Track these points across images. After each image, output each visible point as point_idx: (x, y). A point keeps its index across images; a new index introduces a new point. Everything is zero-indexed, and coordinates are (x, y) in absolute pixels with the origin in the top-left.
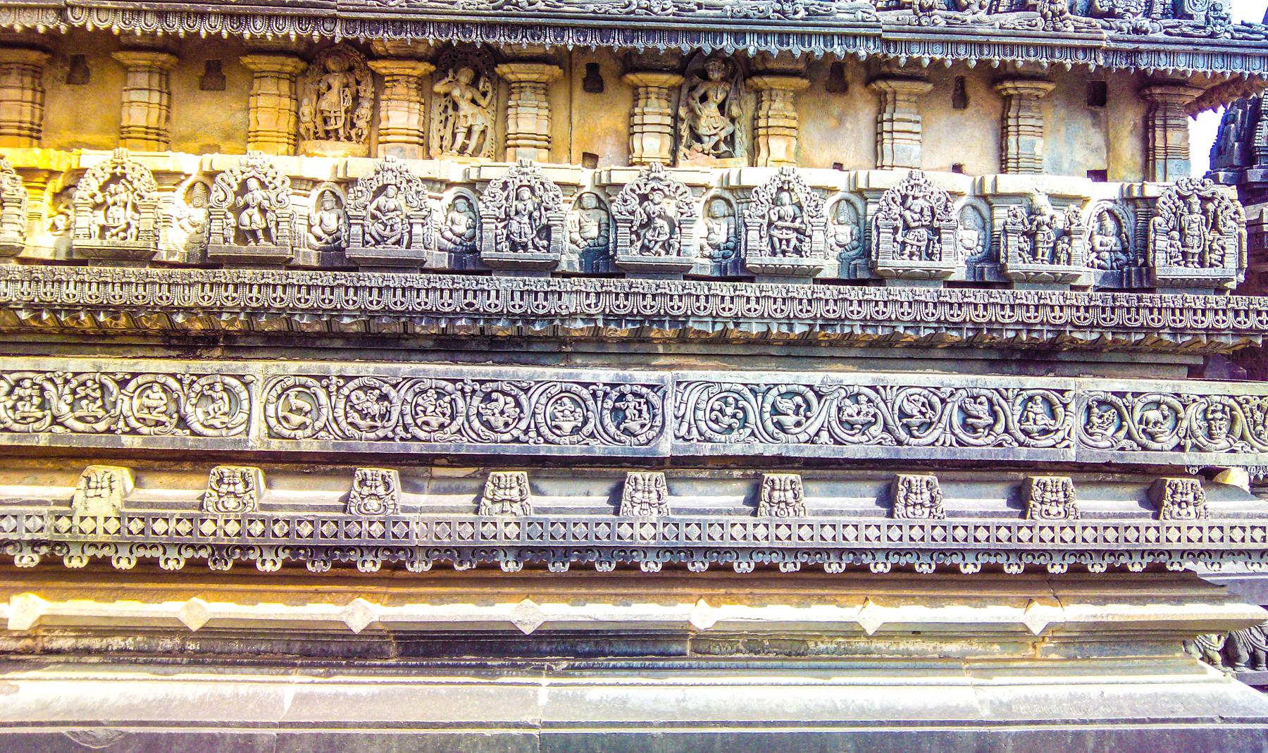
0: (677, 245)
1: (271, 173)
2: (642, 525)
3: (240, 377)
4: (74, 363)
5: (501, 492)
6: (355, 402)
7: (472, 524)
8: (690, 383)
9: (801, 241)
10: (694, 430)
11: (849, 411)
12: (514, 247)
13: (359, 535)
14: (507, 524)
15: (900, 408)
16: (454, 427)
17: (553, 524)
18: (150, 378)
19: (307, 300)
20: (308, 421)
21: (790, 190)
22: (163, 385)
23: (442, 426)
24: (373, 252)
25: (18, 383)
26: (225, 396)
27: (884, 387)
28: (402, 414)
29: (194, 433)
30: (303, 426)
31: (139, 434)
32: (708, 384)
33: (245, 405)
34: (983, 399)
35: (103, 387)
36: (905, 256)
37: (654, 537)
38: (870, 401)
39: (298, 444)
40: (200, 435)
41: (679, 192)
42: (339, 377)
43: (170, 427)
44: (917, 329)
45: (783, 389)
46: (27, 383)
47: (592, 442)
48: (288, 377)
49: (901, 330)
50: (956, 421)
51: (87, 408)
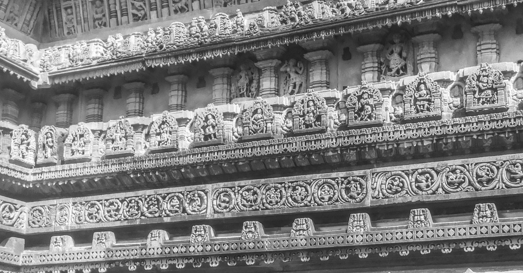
0: (374, 115)
1: (216, 111)
2: (357, 236)
3: (203, 191)
4: (149, 192)
5: (299, 226)
6: (244, 195)
7: (288, 241)
8: (378, 173)
9: (430, 105)
10: (381, 194)
11: (451, 177)
12: (307, 126)
13: (245, 248)
14: (301, 240)
15: (476, 174)
16: (282, 202)
17: (320, 238)
18: (173, 194)
19: (225, 156)
20: (227, 205)
21: (424, 83)
22: (178, 197)
23: (277, 203)
24: (252, 136)
25: (130, 202)
26: (199, 199)
27: (468, 165)
28: (262, 199)
29: (188, 214)
30: (226, 208)
31: (170, 216)
32: (386, 172)
33: (206, 200)
34: (518, 164)
35: (158, 200)
36: (480, 104)
37: (362, 241)
38: (461, 172)
39: (224, 215)
40: (191, 214)
41: (375, 92)
42: (238, 186)
43: (180, 213)
44: (483, 135)
45: (420, 171)
46: (133, 201)
47: (337, 203)
48: (220, 188)
49: (475, 137)
50: (505, 176)
51: (154, 208)
